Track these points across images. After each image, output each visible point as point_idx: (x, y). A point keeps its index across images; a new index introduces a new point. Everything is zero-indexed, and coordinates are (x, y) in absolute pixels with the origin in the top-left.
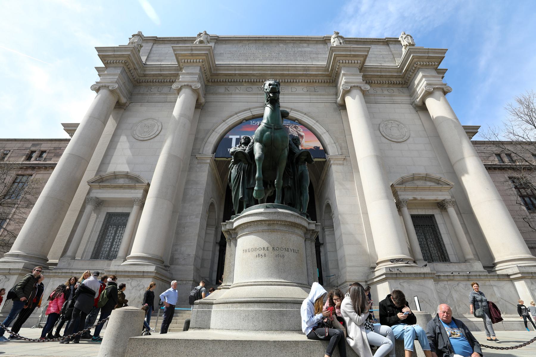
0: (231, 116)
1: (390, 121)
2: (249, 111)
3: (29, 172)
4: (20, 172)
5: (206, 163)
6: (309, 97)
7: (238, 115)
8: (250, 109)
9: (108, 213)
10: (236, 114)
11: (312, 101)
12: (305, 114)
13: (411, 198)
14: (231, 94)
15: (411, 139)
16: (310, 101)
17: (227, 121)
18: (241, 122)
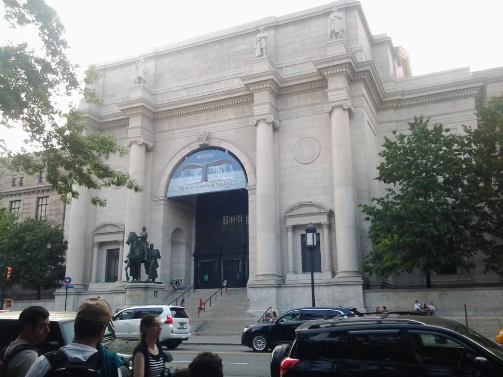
0: (175, 155)
1: (305, 140)
2: (188, 147)
3: (45, 194)
4: (39, 195)
5: (162, 204)
6: (236, 121)
7: (180, 153)
8: (188, 145)
9: (107, 250)
10: (179, 152)
11: (239, 127)
12: (232, 144)
13: (295, 223)
14: (174, 130)
15: (320, 158)
16: (237, 127)
17: (173, 161)
18: (183, 159)
